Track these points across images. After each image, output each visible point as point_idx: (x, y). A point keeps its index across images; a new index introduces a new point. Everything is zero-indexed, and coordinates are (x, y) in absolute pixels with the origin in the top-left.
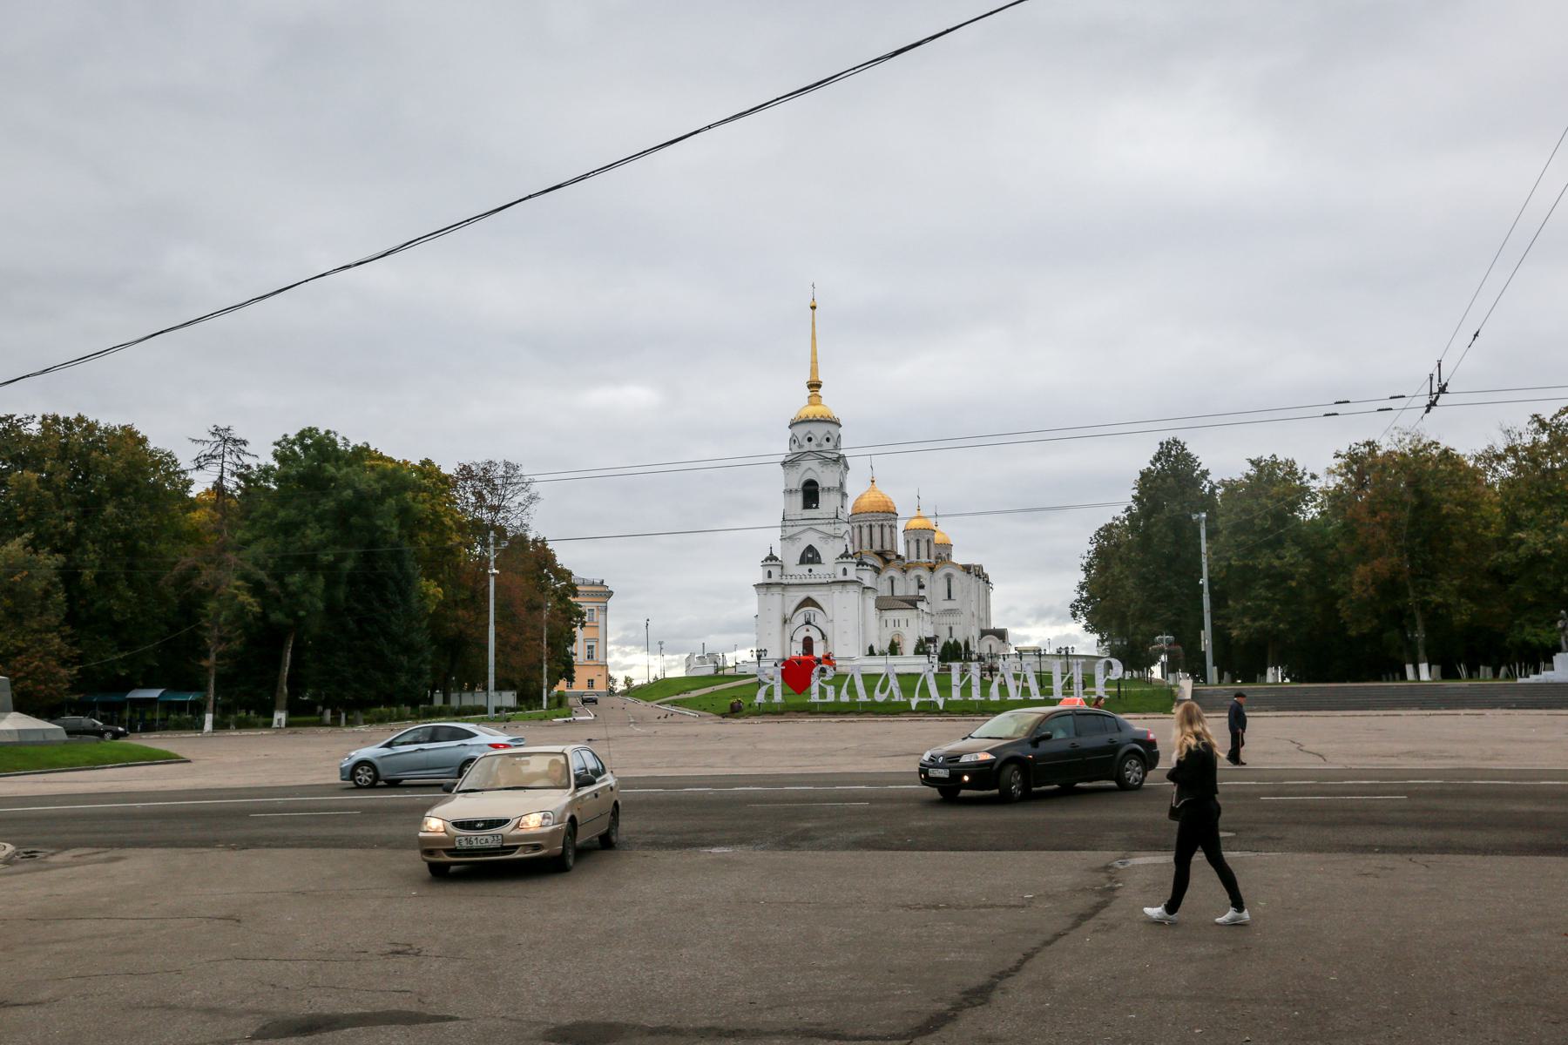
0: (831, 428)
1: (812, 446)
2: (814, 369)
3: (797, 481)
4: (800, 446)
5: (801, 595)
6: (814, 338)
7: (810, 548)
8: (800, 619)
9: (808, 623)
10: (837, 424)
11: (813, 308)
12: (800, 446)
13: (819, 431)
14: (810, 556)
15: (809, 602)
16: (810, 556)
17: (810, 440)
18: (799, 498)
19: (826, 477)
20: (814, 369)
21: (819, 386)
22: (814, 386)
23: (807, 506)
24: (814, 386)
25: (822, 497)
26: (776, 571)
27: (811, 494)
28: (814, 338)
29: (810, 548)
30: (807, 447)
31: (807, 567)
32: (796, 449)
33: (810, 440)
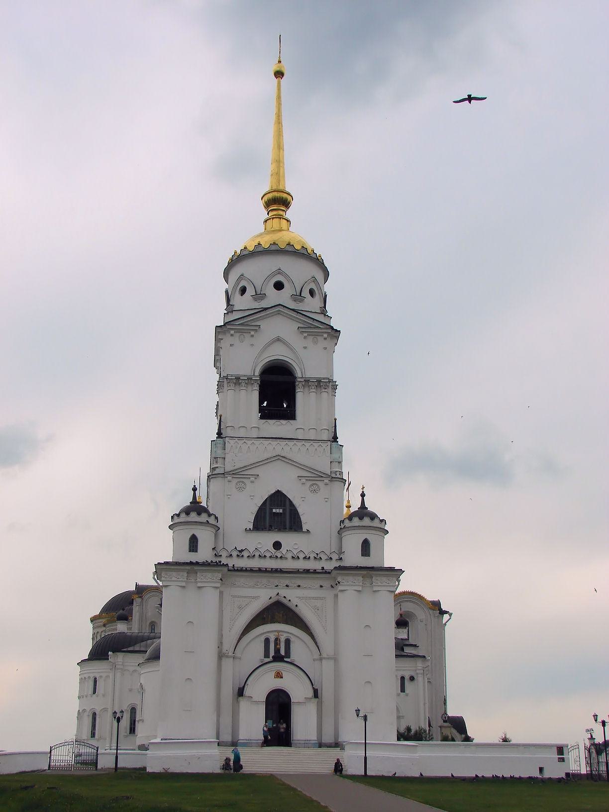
0: (320, 276)
1: (284, 297)
2: (278, 175)
3: (249, 359)
4: (259, 296)
5: (261, 595)
6: (279, 121)
7: (278, 498)
8: (254, 649)
9: (278, 658)
10: (326, 274)
11: (279, 74)
12: (259, 296)
13: (298, 273)
14: (278, 514)
15: (278, 611)
16: (278, 514)
17: (279, 286)
18: (251, 398)
19: (306, 362)
20: (278, 175)
21: (286, 203)
22: (278, 202)
23: (266, 414)
24: (278, 202)
25: (303, 400)
26: (205, 537)
27: (278, 391)
28: (279, 121)
29: (278, 498)
30: (273, 297)
31: (266, 540)
32: (243, 303)
33: (279, 286)
